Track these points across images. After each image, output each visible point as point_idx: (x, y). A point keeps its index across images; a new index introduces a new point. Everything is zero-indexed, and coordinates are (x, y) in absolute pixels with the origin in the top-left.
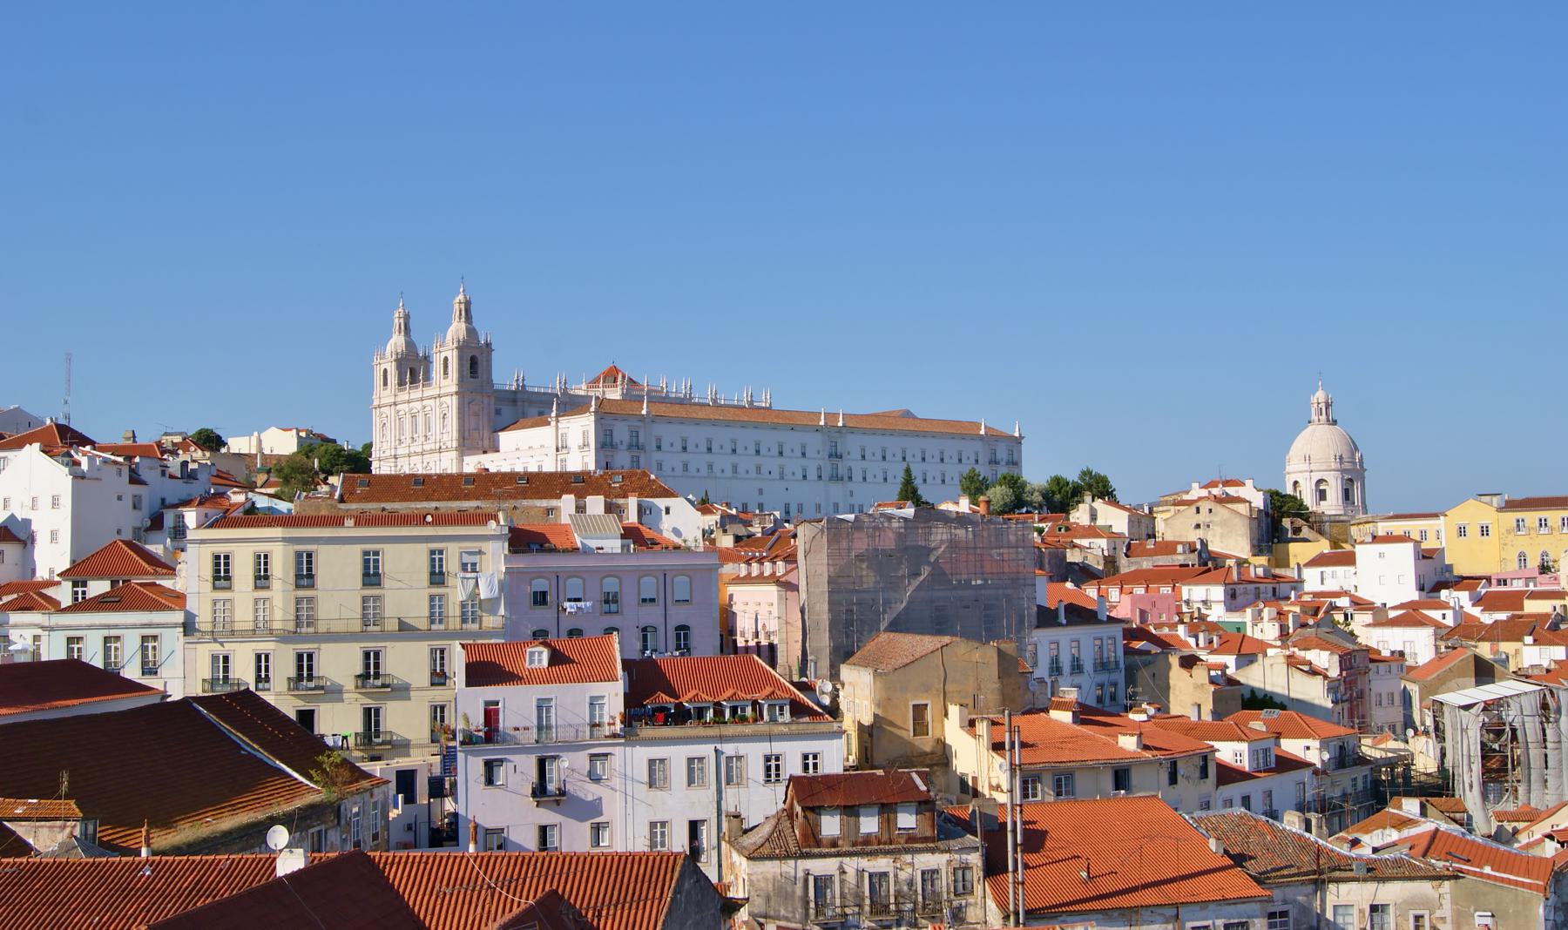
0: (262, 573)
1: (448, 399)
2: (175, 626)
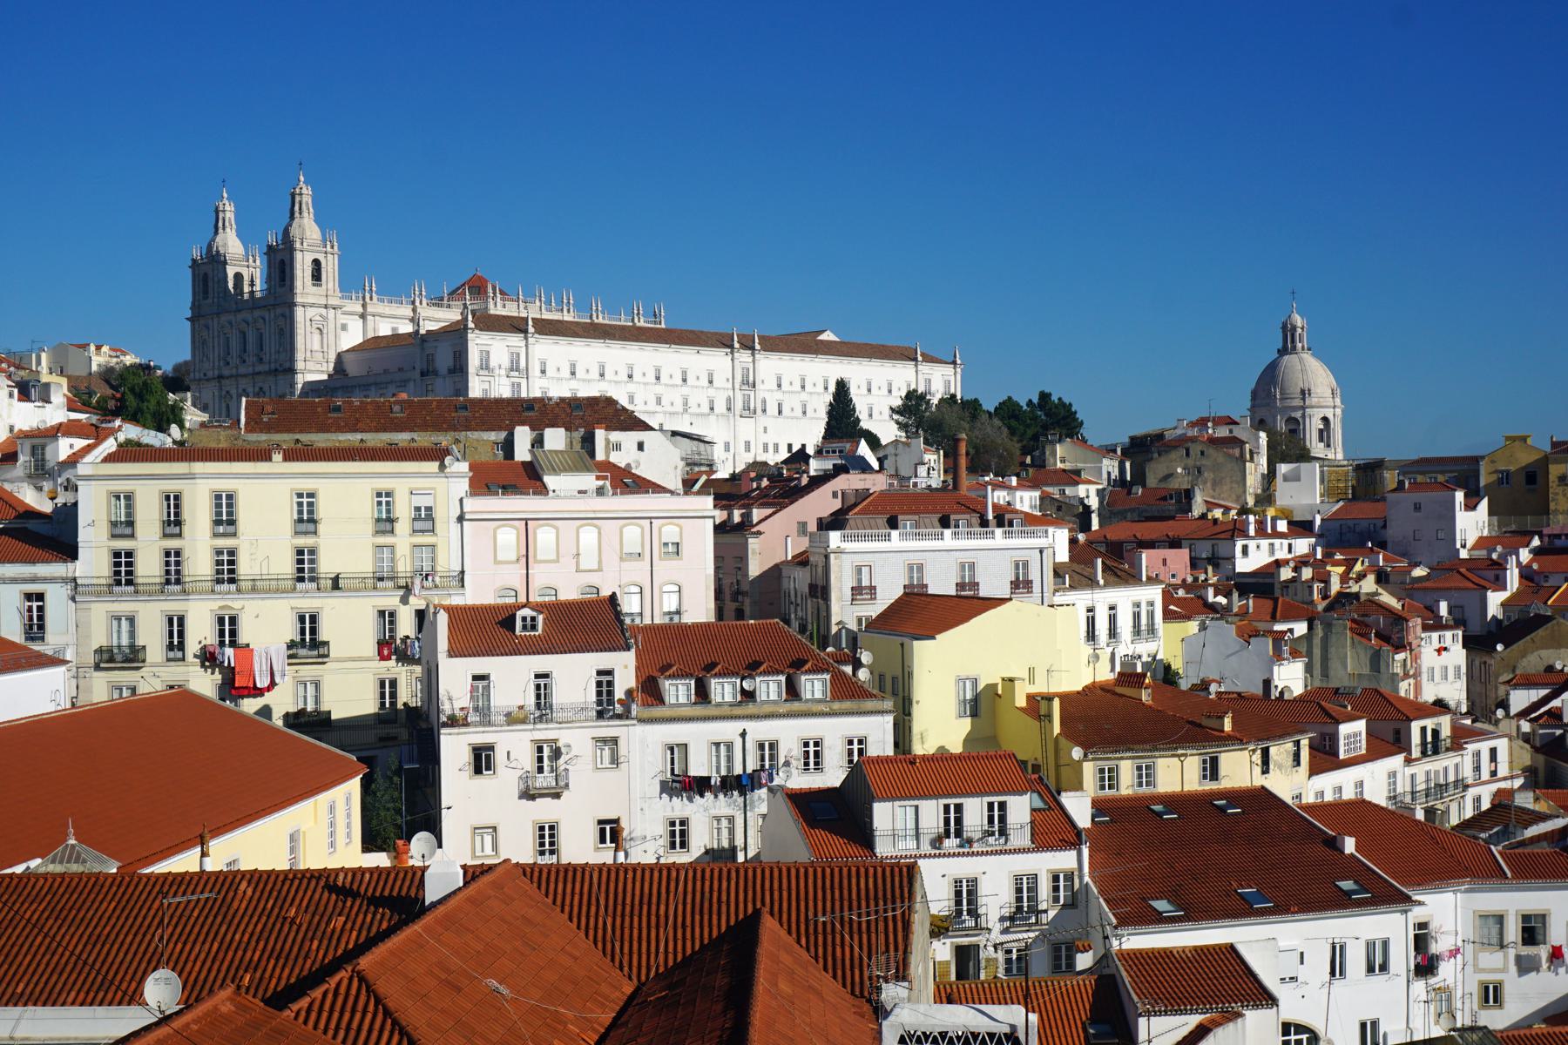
0: (172, 518)
2: (64, 580)
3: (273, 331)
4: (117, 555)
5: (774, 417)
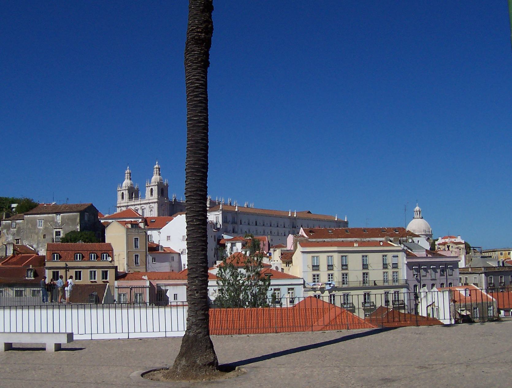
1: (153, 205)
3: (148, 211)
4: (314, 276)
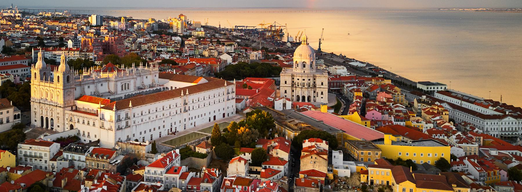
5: (192, 110)
